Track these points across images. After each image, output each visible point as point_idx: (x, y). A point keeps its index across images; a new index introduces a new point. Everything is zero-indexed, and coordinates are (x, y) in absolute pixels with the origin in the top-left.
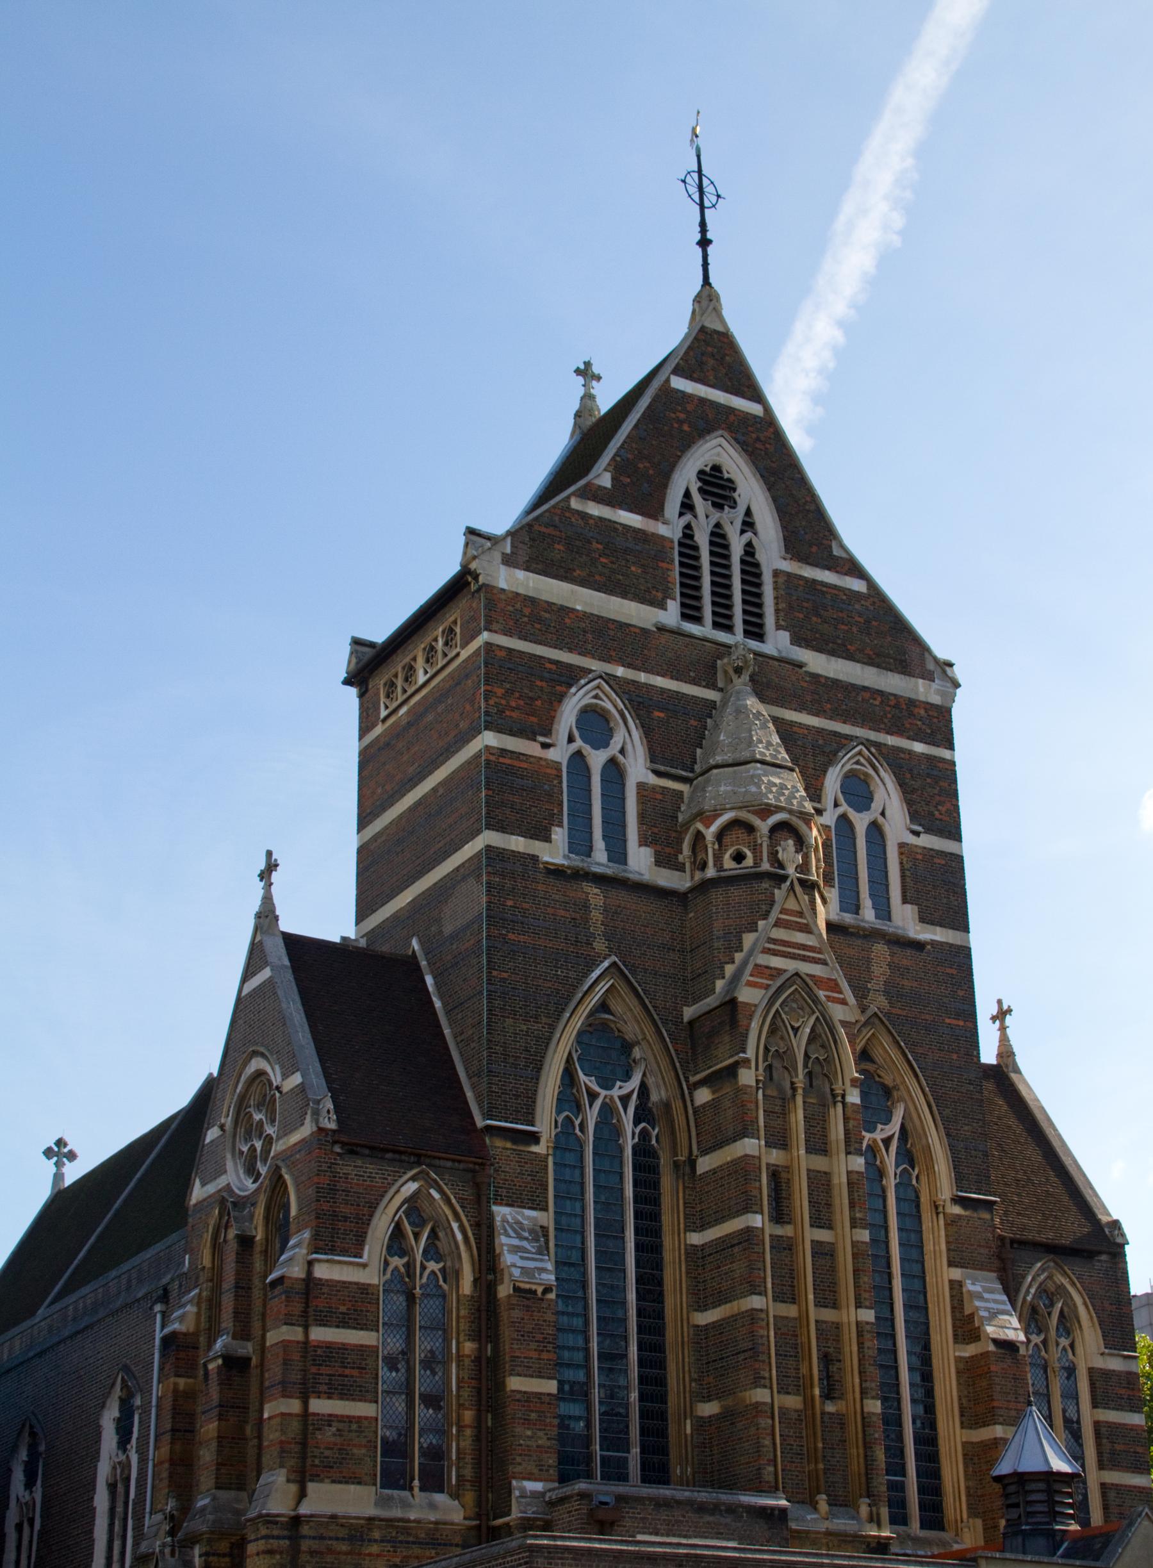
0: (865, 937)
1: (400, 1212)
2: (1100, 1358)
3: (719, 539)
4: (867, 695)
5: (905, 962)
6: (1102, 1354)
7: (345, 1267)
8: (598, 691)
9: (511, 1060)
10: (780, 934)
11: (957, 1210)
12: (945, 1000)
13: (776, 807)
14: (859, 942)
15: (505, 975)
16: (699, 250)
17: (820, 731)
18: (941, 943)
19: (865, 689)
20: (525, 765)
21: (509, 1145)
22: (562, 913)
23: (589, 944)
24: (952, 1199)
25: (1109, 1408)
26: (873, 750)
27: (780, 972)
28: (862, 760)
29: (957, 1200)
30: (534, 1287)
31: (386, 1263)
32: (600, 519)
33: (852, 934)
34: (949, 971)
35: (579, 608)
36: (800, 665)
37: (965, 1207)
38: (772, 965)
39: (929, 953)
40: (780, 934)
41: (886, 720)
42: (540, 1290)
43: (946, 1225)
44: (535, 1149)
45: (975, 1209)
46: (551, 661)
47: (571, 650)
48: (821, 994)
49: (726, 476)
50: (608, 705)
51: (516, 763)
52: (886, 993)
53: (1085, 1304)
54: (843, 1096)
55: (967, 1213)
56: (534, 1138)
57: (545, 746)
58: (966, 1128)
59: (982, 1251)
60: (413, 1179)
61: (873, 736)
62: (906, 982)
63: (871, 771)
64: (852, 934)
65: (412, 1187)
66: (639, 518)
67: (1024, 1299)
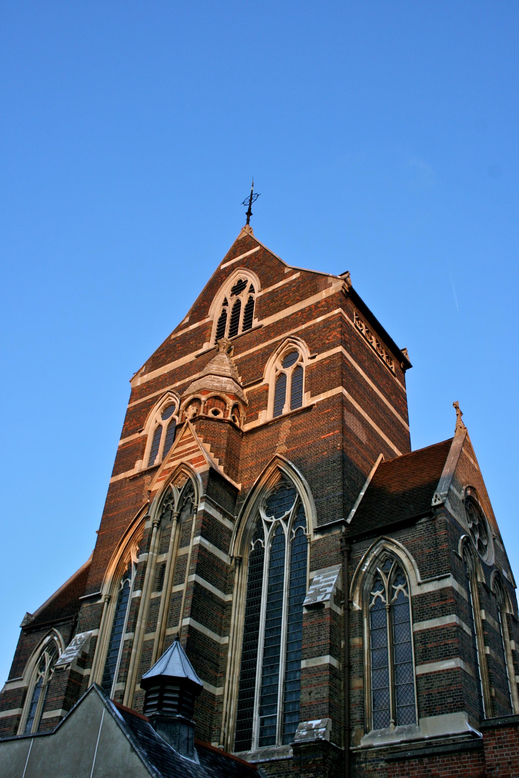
0: (278, 422)
1: (45, 652)
2: (418, 588)
3: (238, 304)
4: (293, 316)
5: (299, 422)
6: (419, 584)
7: (13, 683)
8: (170, 397)
9: (98, 567)
10: (180, 449)
11: (318, 537)
12: (322, 427)
13: (186, 396)
14: (274, 427)
15: (104, 532)
16: (246, 216)
17: (266, 347)
18: (323, 401)
19: (293, 314)
20: (130, 445)
21: (89, 605)
22: (133, 494)
23: (141, 500)
24: (314, 532)
25: (424, 620)
26: (292, 336)
27: (173, 467)
28: (290, 344)
29: (317, 531)
30: (63, 666)
31: (38, 675)
32: (182, 335)
33: (271, 425)
34: (326, 411)
35: (166, 372)
36: (260, 327)
37: (322, 534)
38: (171, 466)
39: (315, 409)
40: (180, 449)
41: (303, 320)
42: (65, 666)
43: (311, 548)
44: (99, 602)
45: (330, 532)
46: (150, 399)
47: (159, 390)
48: (192, 466)
49: (243, 281)
50: (173, 400)
51: (128, 446)
52: (288, 443)
53: (407, 557)
54: (197, 509)
55: (324, 536)
56: (99, 596)
57: (140, 432)
58: (329, 488)
59: (333, 554)
60: (48, 635)
61: (294, 331)
62: (300, 431)
63: (295, 346)
64: (271, 425)
65: (48, 638)
66: (198, 323)
67: (360, 570)
